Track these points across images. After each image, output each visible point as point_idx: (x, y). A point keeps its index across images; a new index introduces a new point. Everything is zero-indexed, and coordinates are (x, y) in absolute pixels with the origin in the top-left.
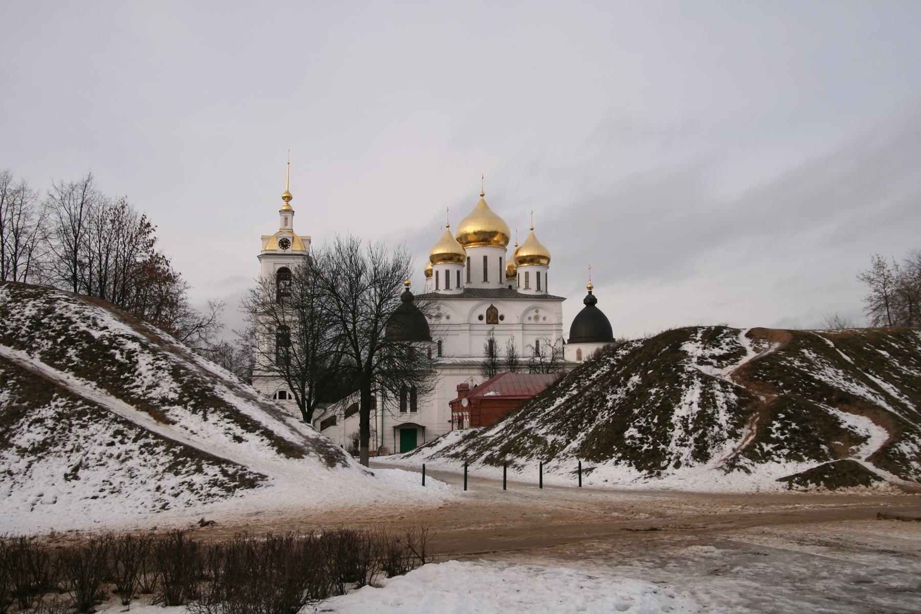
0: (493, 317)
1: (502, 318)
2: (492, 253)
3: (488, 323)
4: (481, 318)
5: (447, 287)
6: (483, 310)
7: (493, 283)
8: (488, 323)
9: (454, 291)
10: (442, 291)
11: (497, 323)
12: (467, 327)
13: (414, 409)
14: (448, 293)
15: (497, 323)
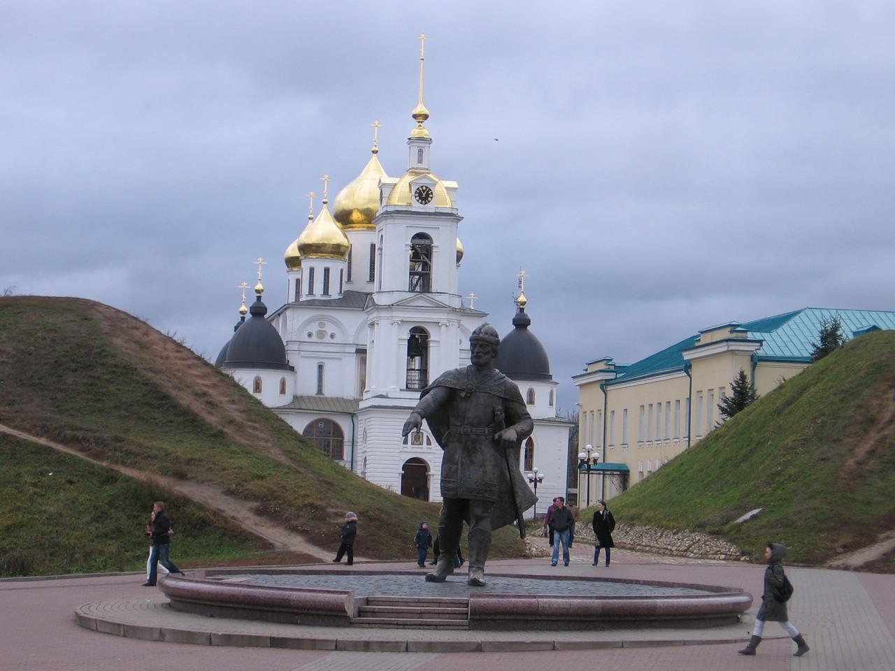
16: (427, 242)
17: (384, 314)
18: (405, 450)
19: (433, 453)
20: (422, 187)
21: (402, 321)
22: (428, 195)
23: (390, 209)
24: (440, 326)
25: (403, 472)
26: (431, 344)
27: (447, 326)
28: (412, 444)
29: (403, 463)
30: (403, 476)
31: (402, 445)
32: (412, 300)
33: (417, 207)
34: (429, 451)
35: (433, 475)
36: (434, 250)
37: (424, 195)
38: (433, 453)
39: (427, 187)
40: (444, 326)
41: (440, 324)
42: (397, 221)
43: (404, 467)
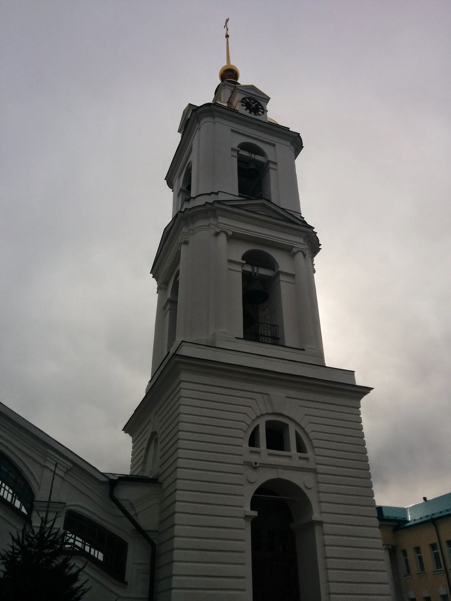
18: (254, 458)
19: (314, 471)
20: (250, 99)
24: (293, 255)
25: (255, 513)
27: (304, 255)
28: (269, 446)
29: (250, 492)
30: (255, 523)
31: (246, 444)
34: (303, 464)
35: (321, 523)
36: (271, 165)
38: (314, 471)
39: (255, 101)
40: (300, 255)
41: (294, 250)
42: (217, 119)
43: (255, 503)
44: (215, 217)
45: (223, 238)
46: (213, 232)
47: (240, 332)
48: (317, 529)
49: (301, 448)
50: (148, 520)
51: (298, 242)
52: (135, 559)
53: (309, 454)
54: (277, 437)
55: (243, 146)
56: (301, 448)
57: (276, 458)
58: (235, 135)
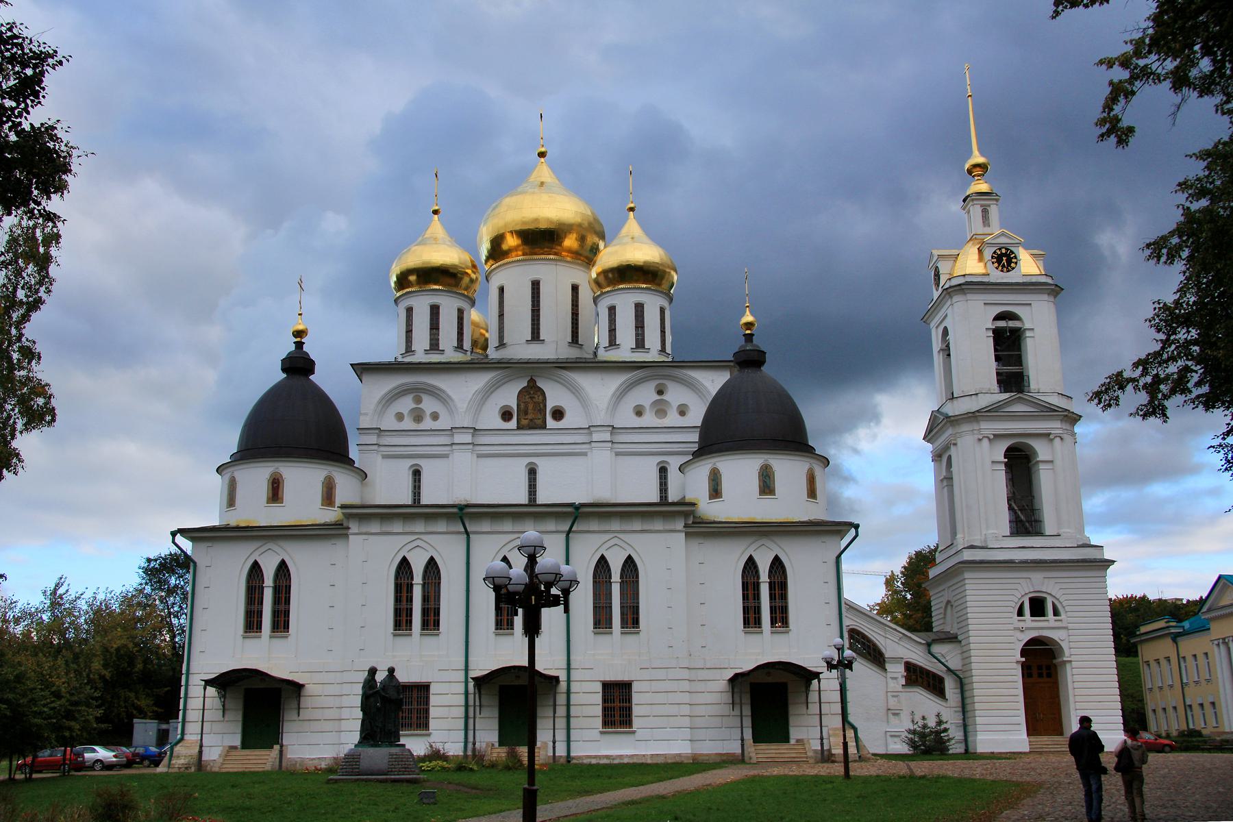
0: (532, 412)
1: (558, 414)
2: (559, 278)
3: (519, 428)
4: (506, 415)
5: (434, 346)
6: (509, 396)
7: (554, 345)
8: (519, 428)
9: (449, 353)
10: (420, 356)
11: (543, 426)
12: (467, 438)
13: (281, 623)
14: (435, 358)
15: (543, 426)
16: (1012, 324)
17: (965, 427)
18: (1021, 624)
21: (995, 435)
22: (1009, 262)
23: (954, 282)
24: (1052, 440)
26: (1041, 466)
28: (1032, 615)
30: (1023, 665)
32: (1008, 403)
33: (997, 276)
36: (1028, 334)
37: (1005, 259)
42: (969, 296)
43: (1024, 653)
44: (978, 422)
45: (985, 441)
46: (977, 437)
47: (1006, 529)
48: (1068, 666)
49: (1056, 613)
50: (954, 663)
51: (1054, 426)
52: (950, 685)
53: (1063, 617)
54: (1037, 607)
55: (999, 317)
56: (1056, 613)
57: (1039, 622)
58: (988, 307)
